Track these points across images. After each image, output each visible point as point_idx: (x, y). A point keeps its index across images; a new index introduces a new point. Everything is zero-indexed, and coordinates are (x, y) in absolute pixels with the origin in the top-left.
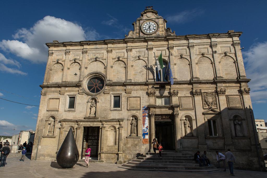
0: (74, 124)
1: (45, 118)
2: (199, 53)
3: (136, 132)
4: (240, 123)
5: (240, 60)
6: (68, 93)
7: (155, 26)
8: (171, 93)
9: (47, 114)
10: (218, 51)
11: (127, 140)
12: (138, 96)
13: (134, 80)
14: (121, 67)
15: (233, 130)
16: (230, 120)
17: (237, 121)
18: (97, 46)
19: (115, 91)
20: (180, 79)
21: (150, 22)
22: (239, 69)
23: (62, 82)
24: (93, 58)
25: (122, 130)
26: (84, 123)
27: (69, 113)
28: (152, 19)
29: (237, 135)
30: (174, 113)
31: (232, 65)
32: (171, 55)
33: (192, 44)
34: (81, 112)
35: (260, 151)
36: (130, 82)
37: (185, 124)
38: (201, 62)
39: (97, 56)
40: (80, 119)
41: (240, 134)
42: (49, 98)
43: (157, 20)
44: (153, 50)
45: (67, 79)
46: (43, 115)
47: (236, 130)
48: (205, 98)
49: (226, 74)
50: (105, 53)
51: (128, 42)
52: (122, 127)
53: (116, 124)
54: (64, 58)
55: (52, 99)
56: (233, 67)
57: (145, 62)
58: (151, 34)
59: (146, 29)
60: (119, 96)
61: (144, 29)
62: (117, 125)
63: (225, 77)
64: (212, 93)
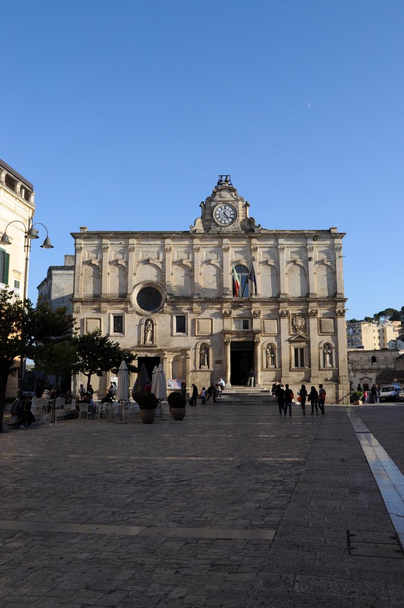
3: (206, 364)
7: (232, 213)
10: (316, 257)
16: (320, 348)
25: (189, 362)
28: (229, 201)
42: (85, 317)
52: (189, 358)
55: (90, 319)
61: (218, 216)
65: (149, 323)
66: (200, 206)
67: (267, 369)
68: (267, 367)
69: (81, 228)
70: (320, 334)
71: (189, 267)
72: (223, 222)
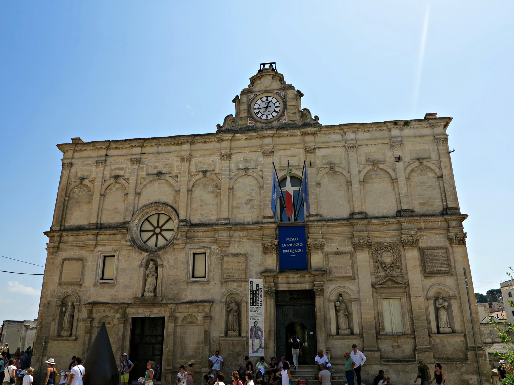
0: (113, 312)
1: (55, 300)
2: (367, 161)
4: (446, 304)
5: (449, 175)
6: (100, 248)
7: (277, 104)
8: (309, 247)
9: (59, 292)
11: (219, 345)
12: (242, 252)
13: (235, 220)
14: (209, 193)
15: (431, 321)
16: (427, 299)
17: (441, 301)
18: (160, 148)
19: (194, 243)
20: (329, 217)
21: (268, 97)
22: (446, 193)
23: (90, 224)
24: (151, 174)
26: (133, 310)
27: (103, 289)
29: (441, 330)
30: (315, 288)
31: (433, 184)
32: (311, 165)
33: (352, 142)
34: (127, 287)
35: (483, 362)
36: (226, 224)
37: (337, 311)
38: (371, 180)
39: (159, 169)
40: (126, 301)
41: (445, 327)
43: (282, 93)
44: (273, 155)
45: (99, 218)
46: (51, 293)
47: (439, 320)
48: (378, 255)
49: (421, 204)
50: (177, 164)
51: (222, 140)
53: (197, 311)
54: (94, 175)
56: (435, 189)
57: (256, 182)
58: (270, 123)
59: (259, 112)
60: (205, 253)
61: (256, 111)
62: (199, 314)
63: (418, 210)
64: (392, 244)
65: (152, 263)
66: (234, 101)
67: (337, 337)
68: (338, 334)
69: (73, 139)
70: (426, 275)
71: (214, 181)
72: (264, 117)
